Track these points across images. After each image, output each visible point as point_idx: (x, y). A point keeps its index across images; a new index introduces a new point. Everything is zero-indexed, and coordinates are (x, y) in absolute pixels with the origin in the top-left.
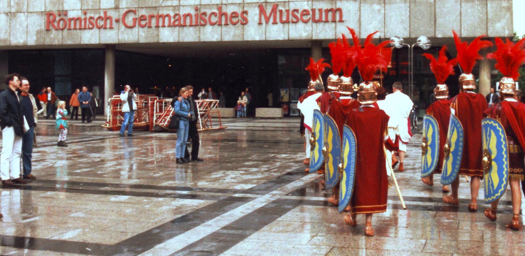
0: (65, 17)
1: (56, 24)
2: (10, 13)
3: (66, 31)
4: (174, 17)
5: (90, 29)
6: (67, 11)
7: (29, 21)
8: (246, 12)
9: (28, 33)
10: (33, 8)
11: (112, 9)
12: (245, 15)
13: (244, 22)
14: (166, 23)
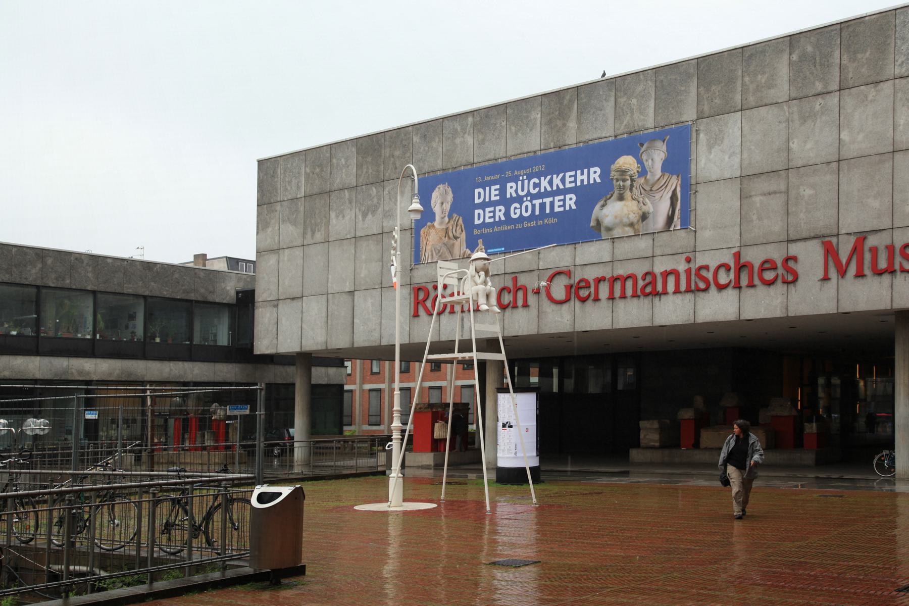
4: (644, 278)
12: (791, 264)
13: (790, 278)
14: (629, 291)
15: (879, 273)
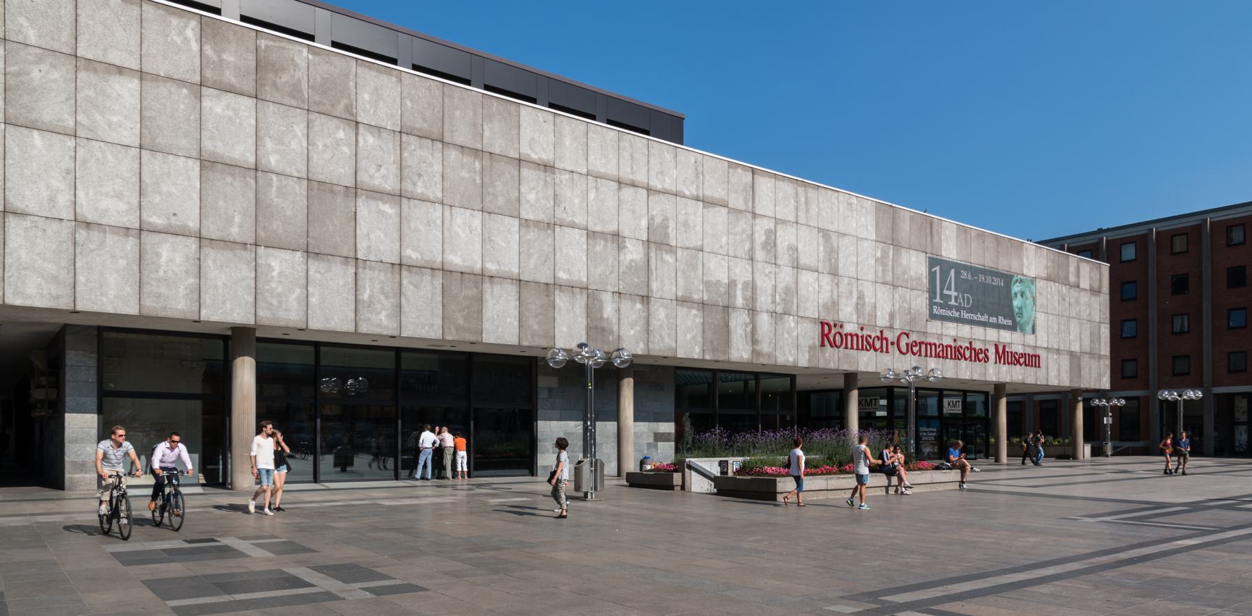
0: (840, 330)
1: (832, 339)
2: (776, 313)
3: (841, 349)
5: (867, 350)
6: (843, 322)
7: (799, 329)
8: (987, 350)
9: (799, 348)
10: (804, 311)
11: (887, 327)
15: (1008, 364)
